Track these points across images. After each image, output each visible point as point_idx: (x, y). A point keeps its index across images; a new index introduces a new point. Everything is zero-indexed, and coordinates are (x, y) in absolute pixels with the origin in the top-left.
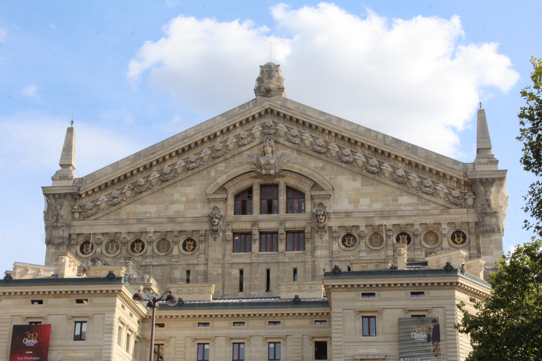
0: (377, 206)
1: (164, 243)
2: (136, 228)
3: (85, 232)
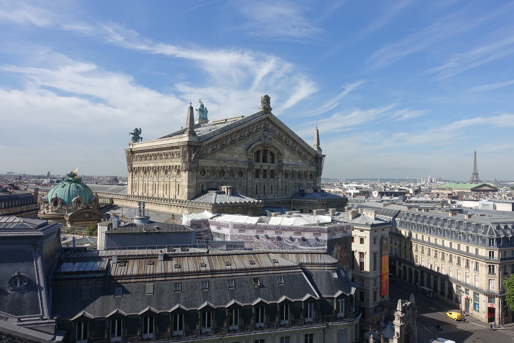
0: (293, 163)
1: (232, 173)
2: (223, 165)
3: (203, 165)
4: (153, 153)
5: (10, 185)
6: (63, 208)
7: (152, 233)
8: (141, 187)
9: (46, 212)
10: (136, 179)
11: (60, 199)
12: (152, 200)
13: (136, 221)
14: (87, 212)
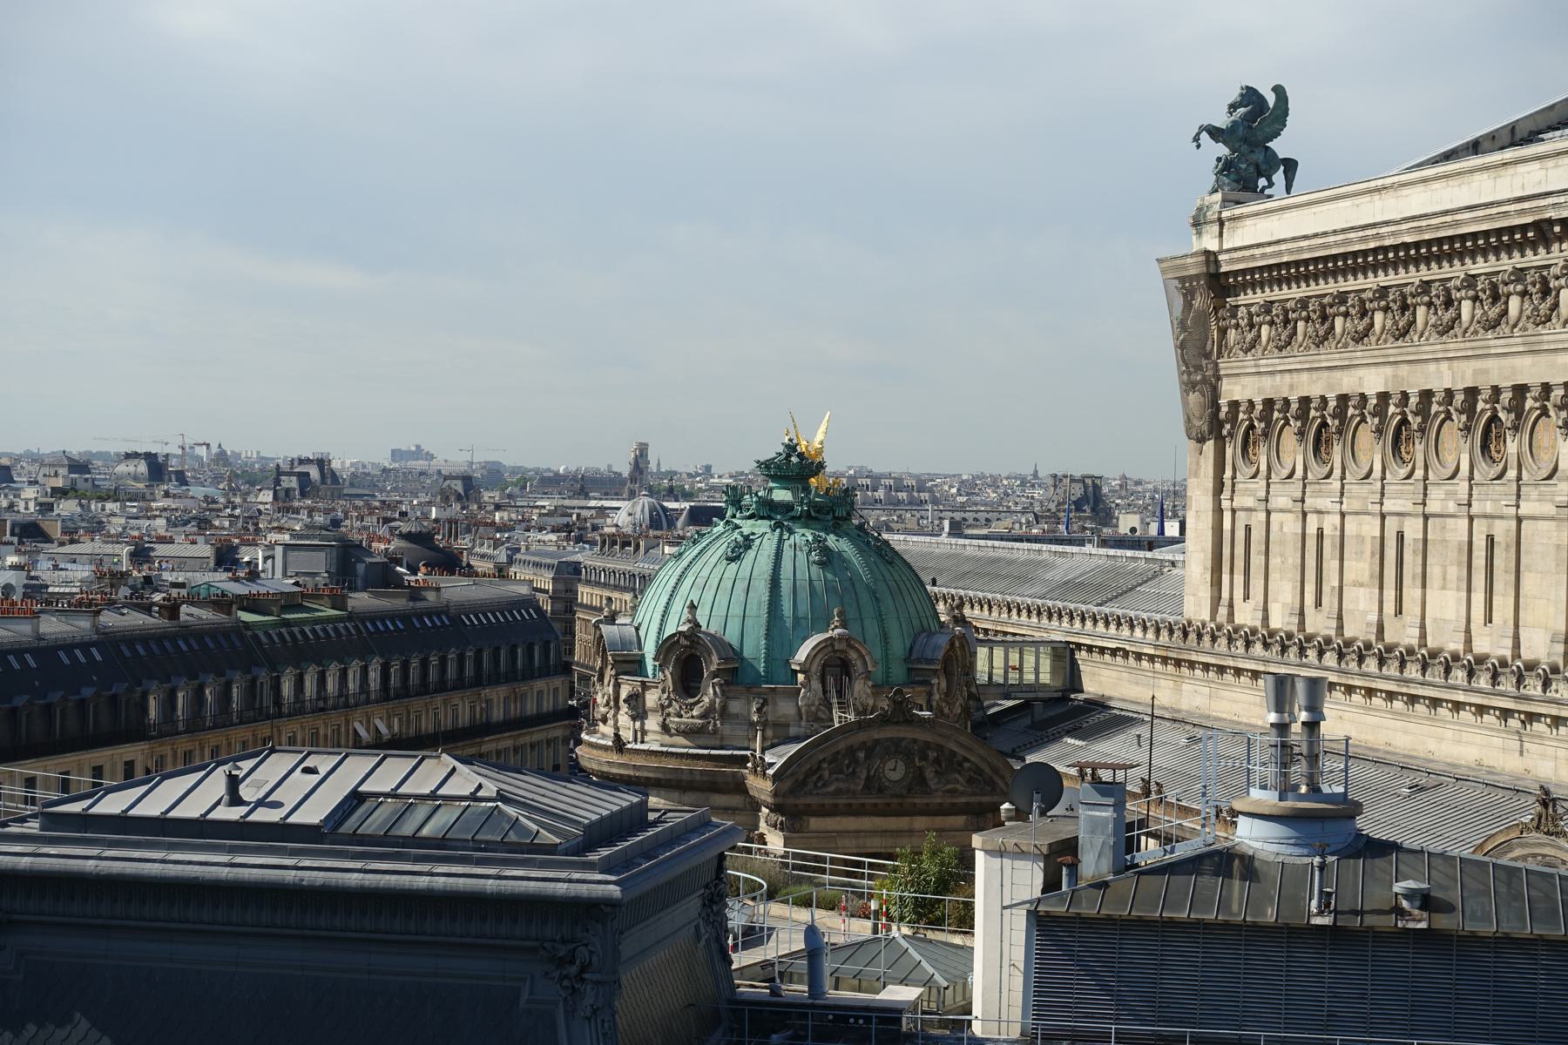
4: (1382, 279)
5: (408, 537)
6: (735, 706)
7: (1378, 936)
8: (1285, 560)
9: (627, 735)
10: (1247, 494)
11: (718, 641)
12: (1371, 665)
13: (1251, 836)
14: (896, 748)
